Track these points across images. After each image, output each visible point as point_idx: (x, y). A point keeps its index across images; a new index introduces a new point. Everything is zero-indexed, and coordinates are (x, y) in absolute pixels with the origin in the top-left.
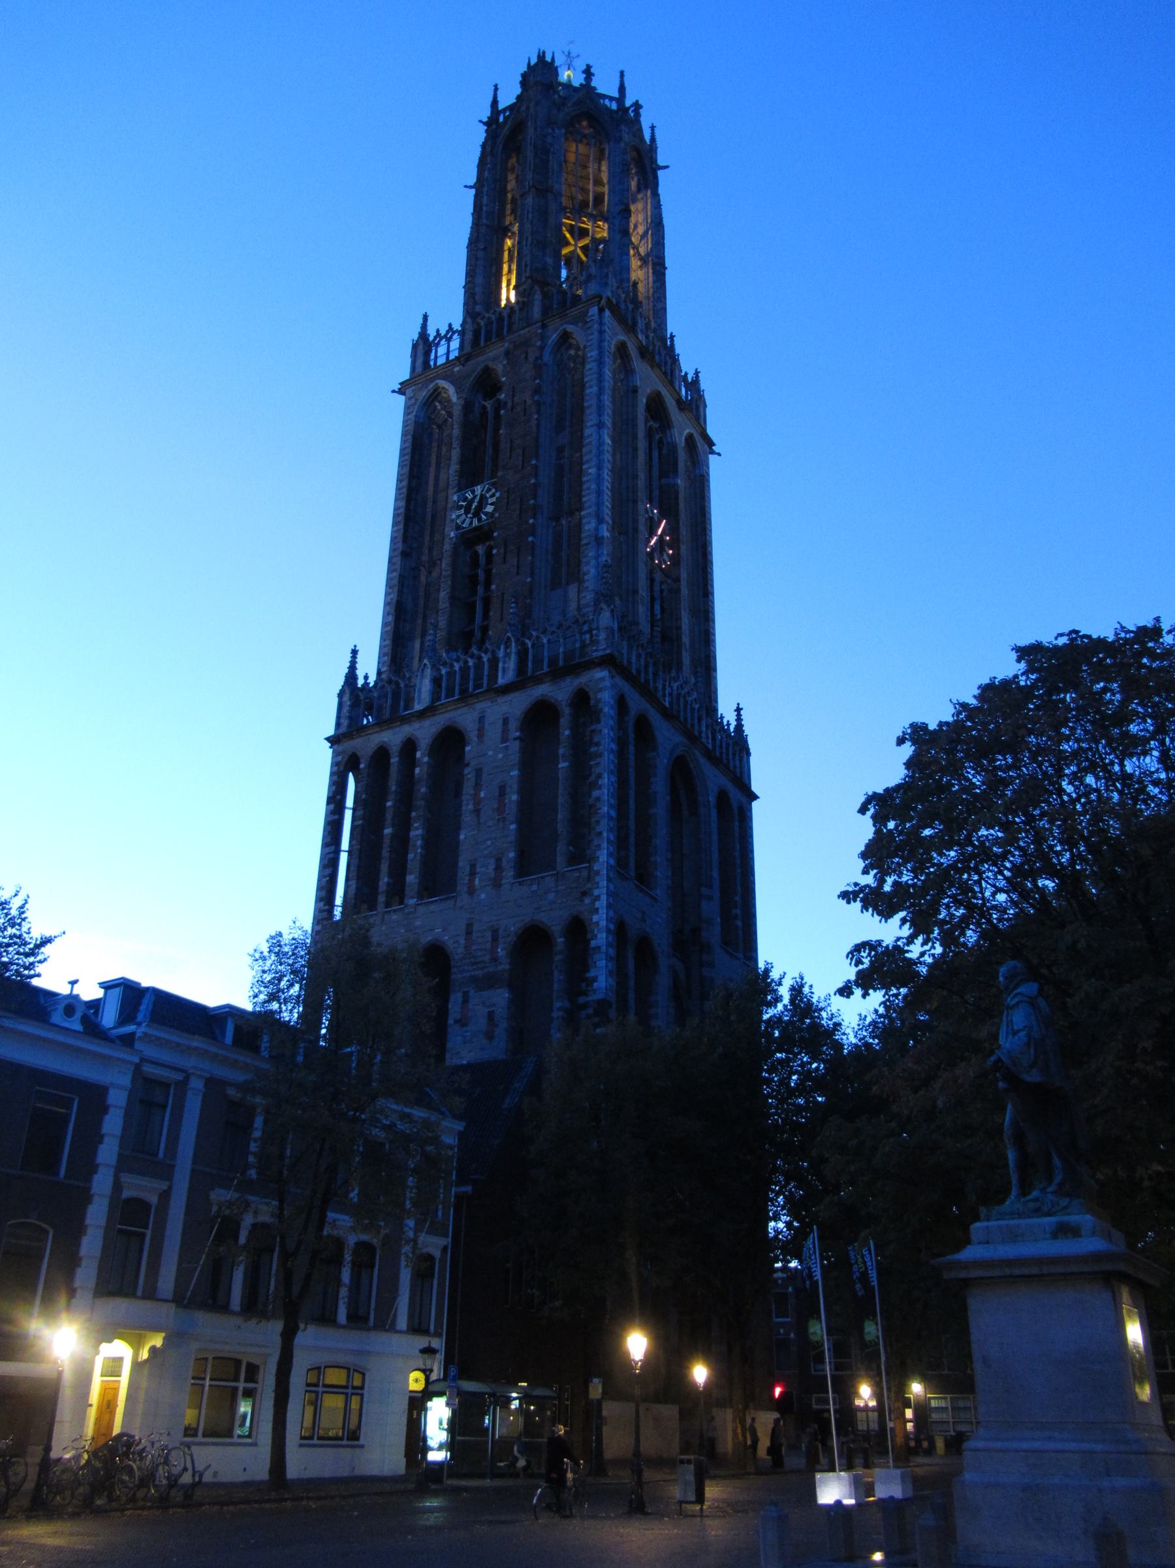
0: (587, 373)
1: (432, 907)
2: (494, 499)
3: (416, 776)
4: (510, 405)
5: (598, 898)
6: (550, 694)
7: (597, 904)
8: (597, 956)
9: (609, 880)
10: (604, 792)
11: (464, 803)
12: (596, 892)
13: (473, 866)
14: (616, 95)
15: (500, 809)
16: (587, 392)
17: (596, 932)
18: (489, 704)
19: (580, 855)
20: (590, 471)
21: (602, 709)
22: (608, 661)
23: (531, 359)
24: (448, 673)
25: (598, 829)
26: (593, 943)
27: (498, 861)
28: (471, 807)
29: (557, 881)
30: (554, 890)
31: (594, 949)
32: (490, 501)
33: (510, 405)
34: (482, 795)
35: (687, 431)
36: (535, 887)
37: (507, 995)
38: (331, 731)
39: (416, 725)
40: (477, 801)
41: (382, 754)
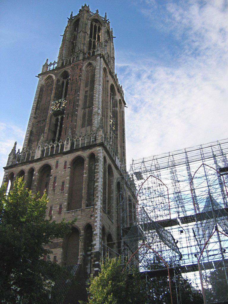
2: (65, 103)
4: (72, 79)
5: (97, 217)
6: (81, 154)
7: (96, 219)
8: (95, 237)
9: (100, 212)
10: (100, 184)
11: (50, 187)
12: (96, 215)
14: (104, 17)
17: (96, 228)
18: (60, 157)
19: (91, 203)
22: (102, 145)
23: (79, 68)
24: (47, 149)
26: (94, 232)
27: (61, 205)
28: (52, 189)
30: (80, 215)
31: (95, 234)
32: (64, 103)
33: (72, 79)
34: (56, 185)
35: (119, 98)
36: (73, 214)
37: (61, 250)
38: (5, 166)
39: (34, 164)
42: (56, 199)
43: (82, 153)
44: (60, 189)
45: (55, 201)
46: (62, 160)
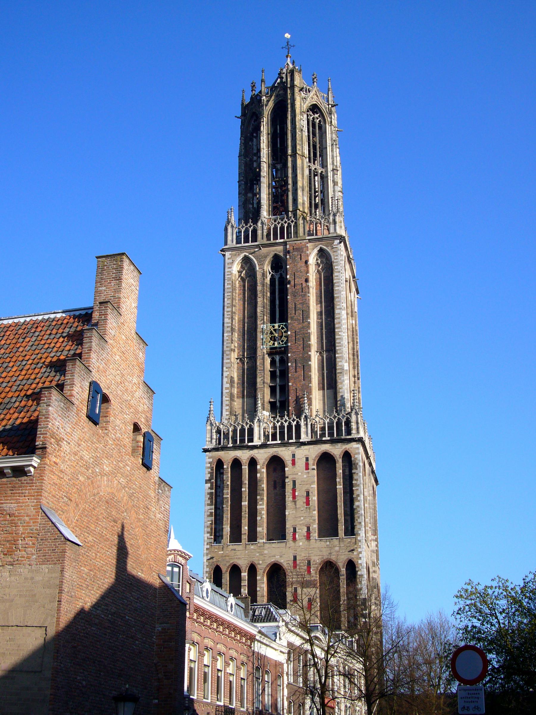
1: (273, 545)
3: (258, 478)
4: (292, 283)
6: (330, 450)
11: (287, 496)
13: (295, 529)
15: (308, 503)
19: (351, 531)
21: (358, 463)
25: (359, 521)
26: (359, 573)
27: (308, 528)
29: (339, 542)
30: (338, 546)
31: (359, 575)
34: (297, 494)
36: (328, 543)
40: (294, 497)
41: (236, 464)
42: (300, 517)
43: (331, 447)
44: (304, 503)
45: (299, 519)
46: (302, 453)
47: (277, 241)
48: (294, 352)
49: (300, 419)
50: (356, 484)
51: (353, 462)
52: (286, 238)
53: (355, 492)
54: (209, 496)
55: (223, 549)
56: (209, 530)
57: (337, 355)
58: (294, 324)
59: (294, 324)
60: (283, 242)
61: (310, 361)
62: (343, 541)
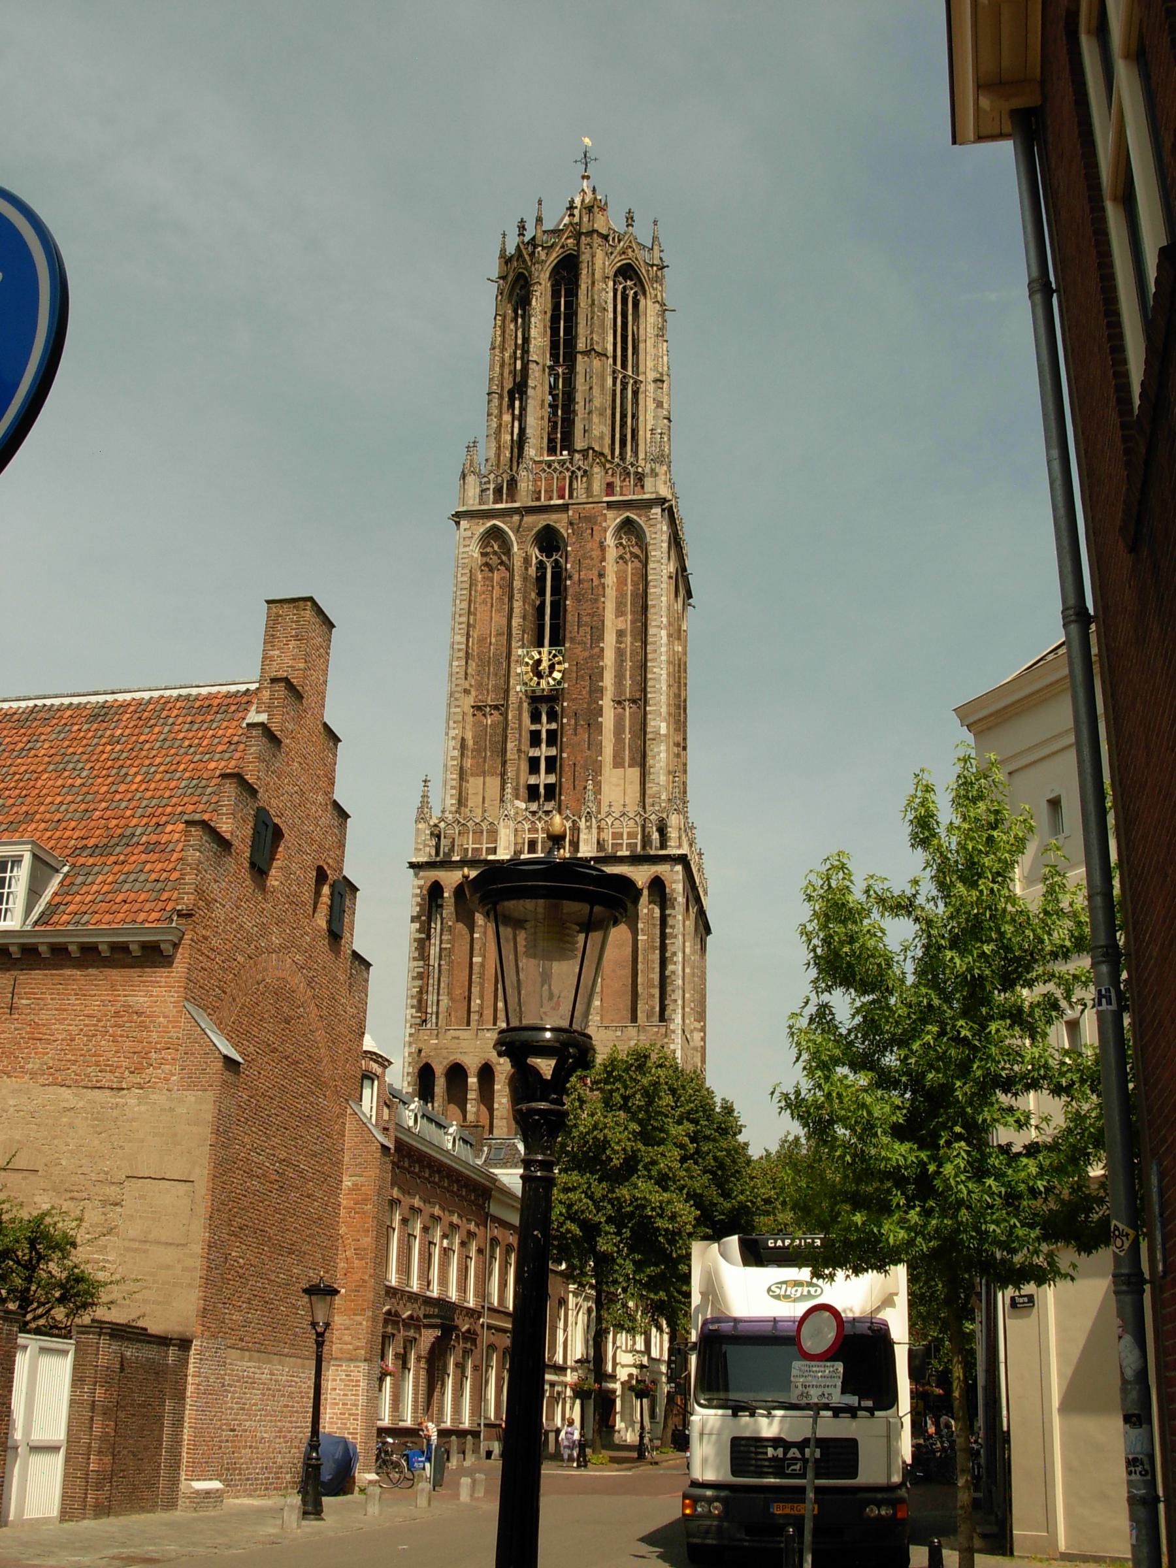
0: (651, 572)
4: (576, 577)
16: (652, 590)
20: (655, 670)
25: (673, 997)
36: (619, 1033)
47: (552, 502)
48: (573, 700)
49: (580, 818)
50: (671, 933)
51: (668, 896)
52: (567, 497)
53: (668, 948)
54: (416, 944)
55: (437, 1035)
56: (415, 1002)
57: (648, 708)
58: (575, 651)
59: (575, 651)
60: (563, 505)
61: (601, 716)
62: (645, 1031)
